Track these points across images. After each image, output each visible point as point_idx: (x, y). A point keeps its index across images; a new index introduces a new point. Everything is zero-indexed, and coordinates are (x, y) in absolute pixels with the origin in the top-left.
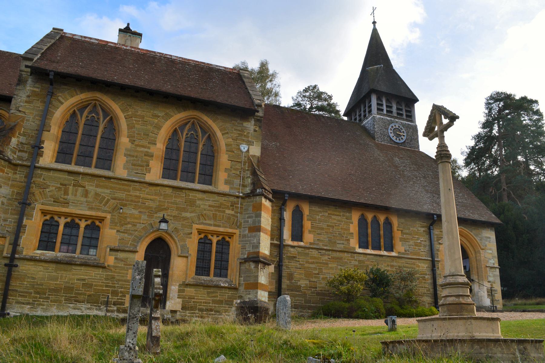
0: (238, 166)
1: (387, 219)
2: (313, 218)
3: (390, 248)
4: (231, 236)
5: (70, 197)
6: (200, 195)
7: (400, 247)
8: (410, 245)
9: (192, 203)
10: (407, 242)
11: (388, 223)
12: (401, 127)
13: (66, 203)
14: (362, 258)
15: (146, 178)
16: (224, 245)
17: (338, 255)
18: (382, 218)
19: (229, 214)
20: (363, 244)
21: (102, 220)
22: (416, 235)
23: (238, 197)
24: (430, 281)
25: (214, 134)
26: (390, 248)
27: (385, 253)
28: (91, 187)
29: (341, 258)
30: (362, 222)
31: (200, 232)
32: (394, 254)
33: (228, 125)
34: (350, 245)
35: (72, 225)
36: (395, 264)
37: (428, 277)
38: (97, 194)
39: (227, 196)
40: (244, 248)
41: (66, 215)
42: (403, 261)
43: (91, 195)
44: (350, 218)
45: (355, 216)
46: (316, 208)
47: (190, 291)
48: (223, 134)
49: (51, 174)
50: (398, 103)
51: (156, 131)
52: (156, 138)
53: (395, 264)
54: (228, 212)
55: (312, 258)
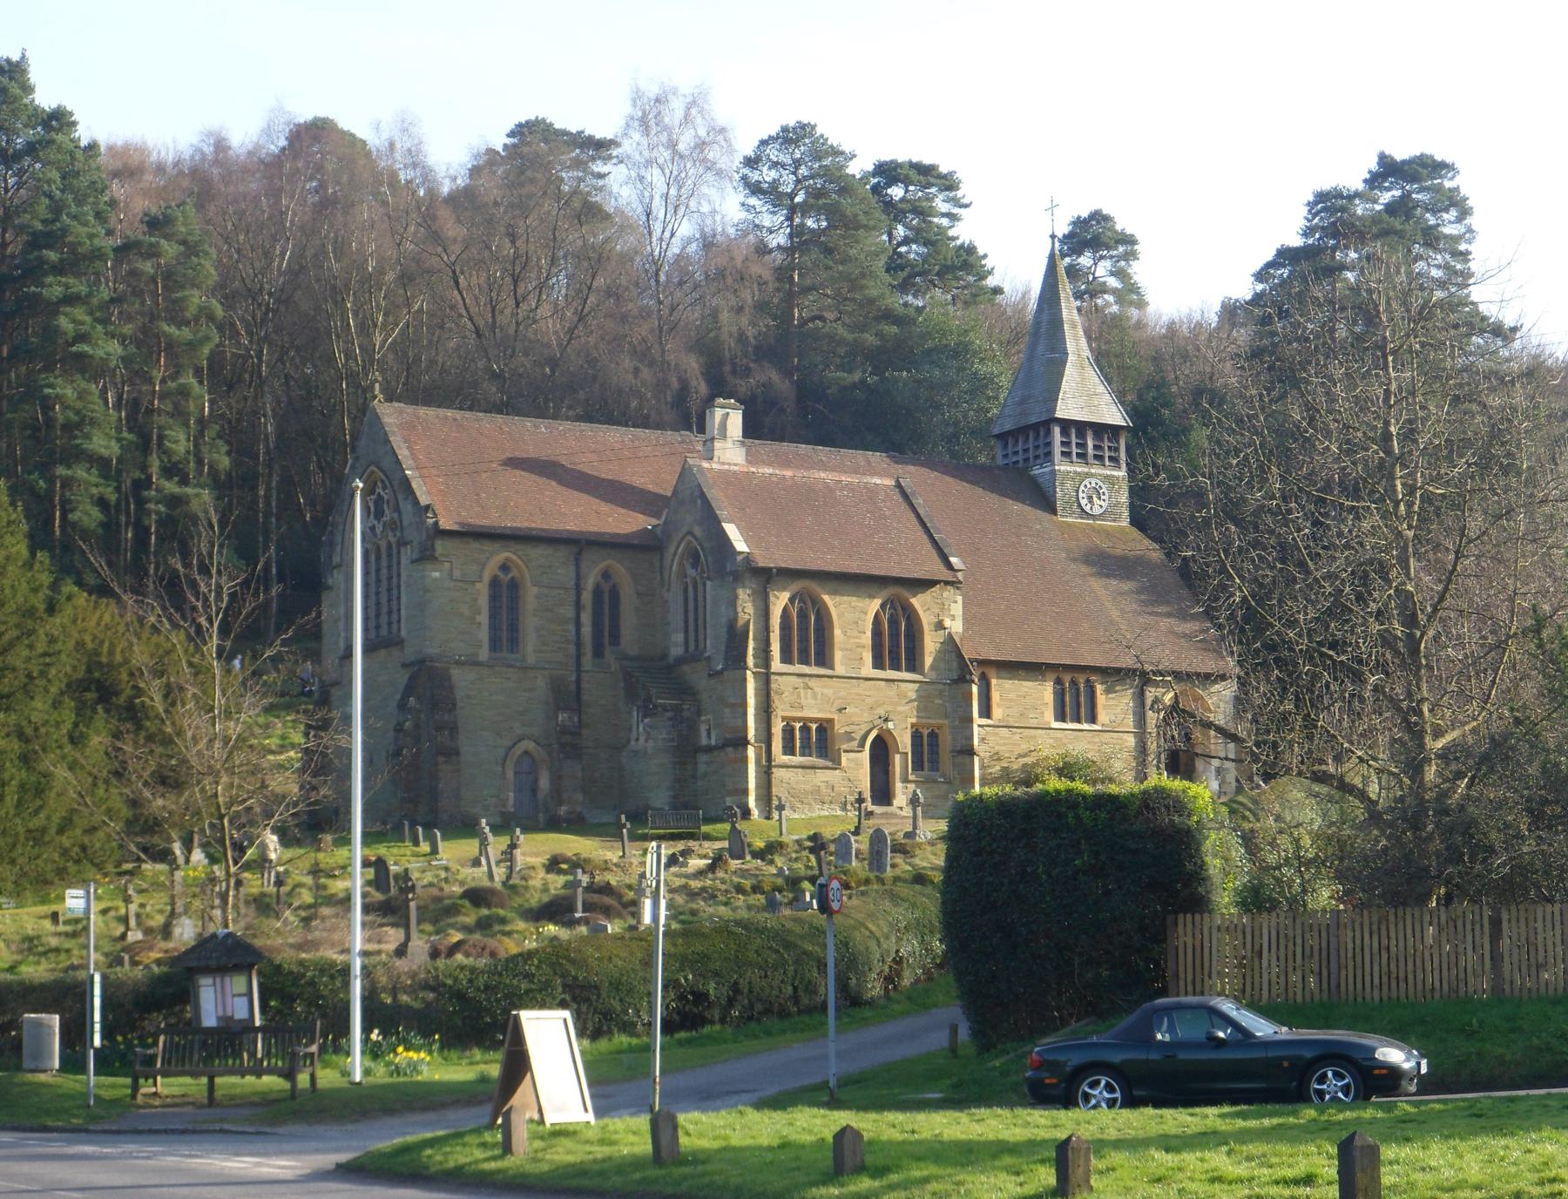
1: (1088, 681)
3: (1093, 719)
5: (803, 701)
7: (1103, 716)
12: (1100, 483)
14: (1059, 734)
16: (933, 736)
18: (1081, 680)
20: (1061, 716)
26: (1093, 719)
27: (1086, 726)
32: (1096, 727)
35: (805, 729)
36: (1096, 740)
40: (954, 739)
42: (1107, 735)
43: (819, 696)
51: (862, 616)
53: (1096, 740)
55: (1002, 738)
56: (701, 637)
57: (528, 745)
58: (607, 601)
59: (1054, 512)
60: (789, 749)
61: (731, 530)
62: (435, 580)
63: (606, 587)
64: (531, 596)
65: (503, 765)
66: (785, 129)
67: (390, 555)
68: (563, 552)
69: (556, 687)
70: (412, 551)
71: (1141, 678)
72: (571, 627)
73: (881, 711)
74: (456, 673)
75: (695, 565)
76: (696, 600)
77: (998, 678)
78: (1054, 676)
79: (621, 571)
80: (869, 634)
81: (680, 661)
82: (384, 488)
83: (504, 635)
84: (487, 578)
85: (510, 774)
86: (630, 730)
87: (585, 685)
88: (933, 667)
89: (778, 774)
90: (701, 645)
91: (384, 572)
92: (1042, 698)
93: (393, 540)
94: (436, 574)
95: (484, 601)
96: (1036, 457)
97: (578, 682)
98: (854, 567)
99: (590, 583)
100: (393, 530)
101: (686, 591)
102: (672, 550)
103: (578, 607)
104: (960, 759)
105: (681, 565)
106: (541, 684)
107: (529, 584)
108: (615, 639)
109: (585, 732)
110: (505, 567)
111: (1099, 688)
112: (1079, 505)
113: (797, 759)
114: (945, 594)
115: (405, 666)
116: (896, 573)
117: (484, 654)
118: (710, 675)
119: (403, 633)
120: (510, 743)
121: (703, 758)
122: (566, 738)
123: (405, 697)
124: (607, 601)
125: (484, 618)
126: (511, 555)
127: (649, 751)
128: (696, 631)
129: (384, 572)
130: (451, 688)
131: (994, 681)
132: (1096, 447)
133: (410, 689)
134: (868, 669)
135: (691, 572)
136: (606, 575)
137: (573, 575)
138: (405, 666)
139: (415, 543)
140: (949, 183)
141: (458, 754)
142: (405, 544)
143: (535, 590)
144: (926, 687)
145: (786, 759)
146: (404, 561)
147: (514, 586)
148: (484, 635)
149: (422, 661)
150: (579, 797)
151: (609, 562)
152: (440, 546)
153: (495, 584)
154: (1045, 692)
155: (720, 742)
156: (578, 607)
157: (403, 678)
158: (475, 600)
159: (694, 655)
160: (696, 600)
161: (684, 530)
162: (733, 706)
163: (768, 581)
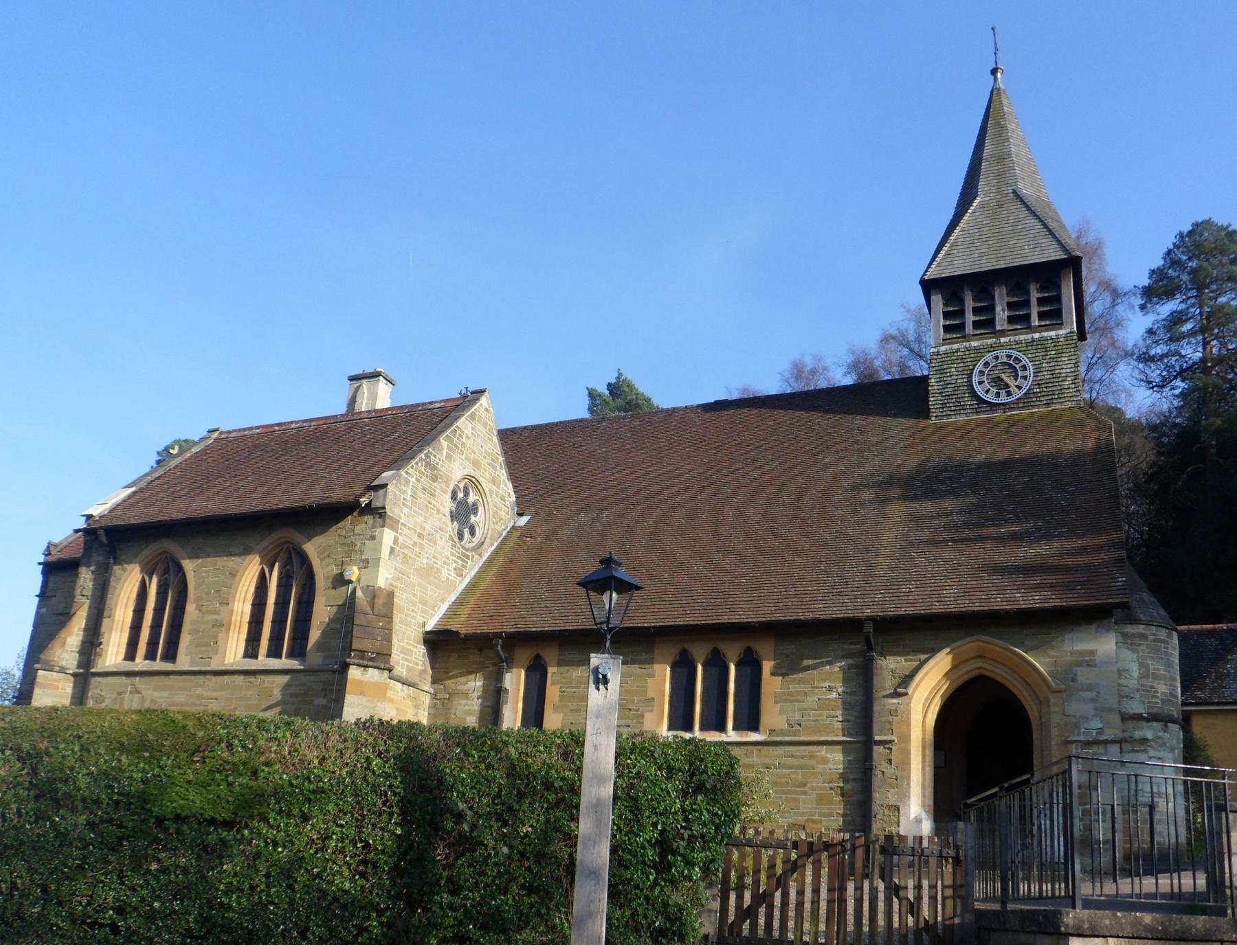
2: (564, 678)
8: (805, 709)
10: (797, 701)
15: (212, 664)
19: (318, 706)
22: (824, 680)
23: (334, 672)
34: (641, 727)
39: (319, 673)
48: (322, 560)
52: (229, 594)
59: (924, 412)
77: (561, 663)
78: (672, 651)
88: (320, 646)
111: (767, 666)
112: (974, 395)
114: (358, 529)
131: (551, 670)
144: (303, 678)
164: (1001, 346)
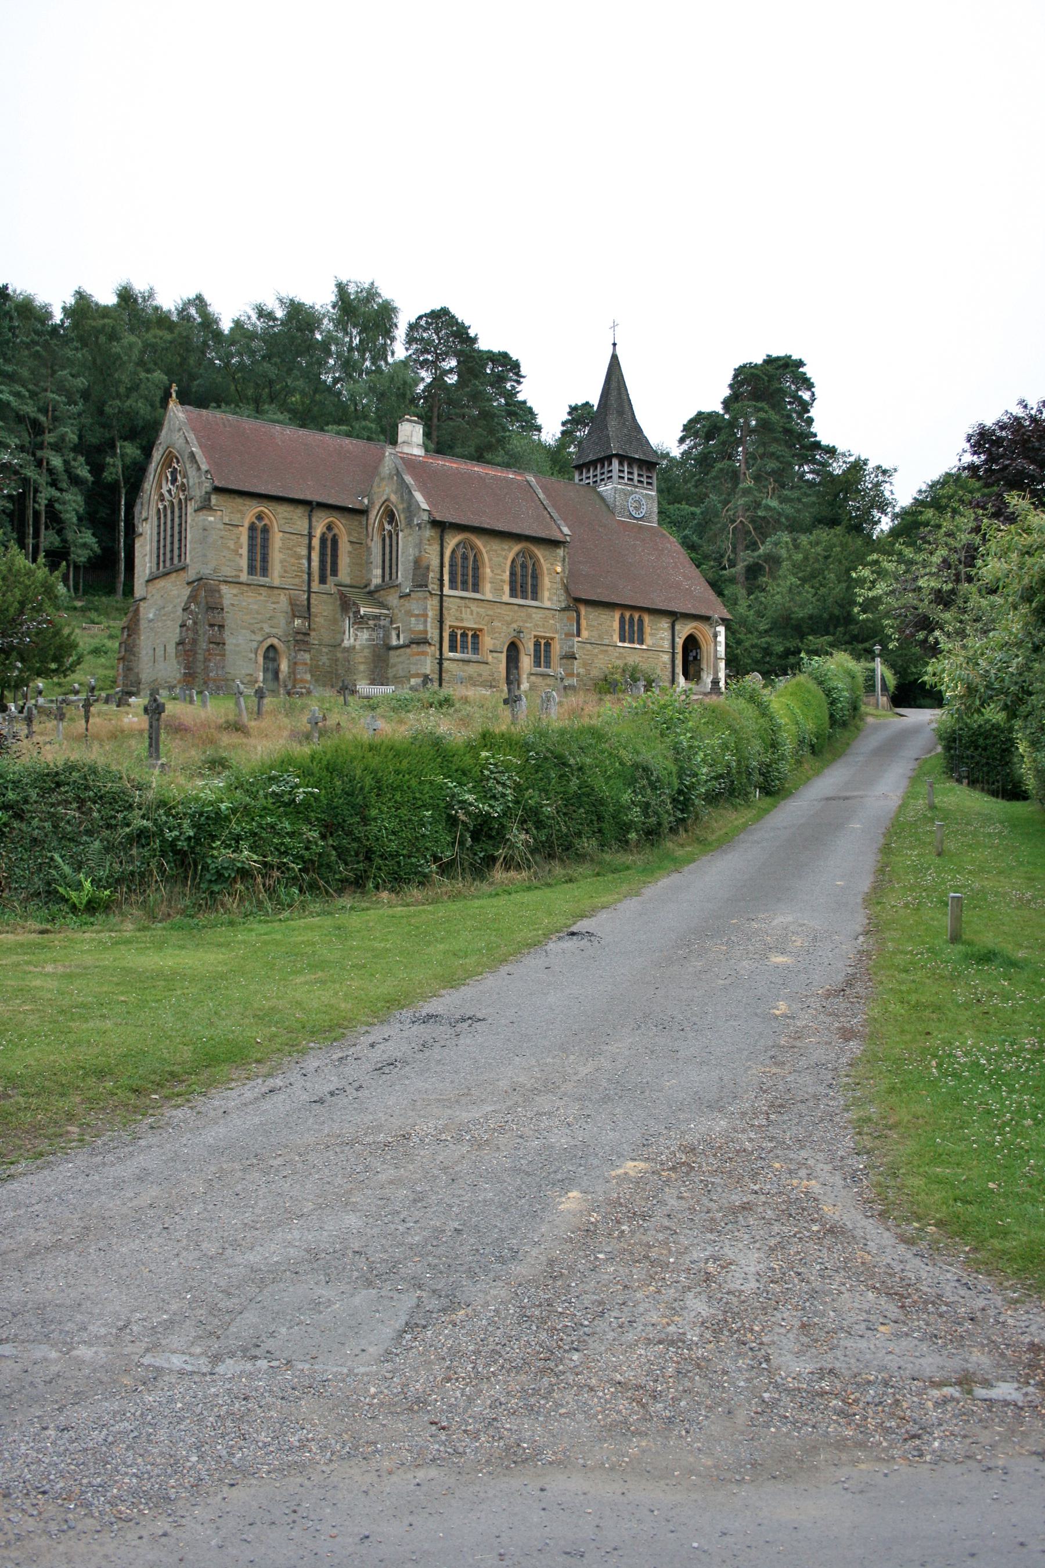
0: (555, 586)
3: (641, 642)
4: (552, 639)
5: (464, 616)
6: (534, 610)
7: (649, 640)
9: (529, 616)
11: (641, 621)
13: (462, 620)
14: (622, 650)
16: (548, 645)
17: (605, 648)
18: (636, 617)
20: (622, 639)
21: (481, 630)
24: (670, 670)
25: (538, 560)
26: (641, 642)
27: (638, 646)
28: (473, 607)
29: (606, 651)
30: (622, 617)
31: (535, 637)
32: (644, 647)
33: (547, 553)
37: (669, 666)
38: (478, 613)
40: (561, 648)
41: (461, 628)
44: (613, 617)
45: (617, 615)
46: (590, 609)
47: (533, 678)
49: (451, 599)
50: (640, 468)
54: (551, 622)
56: (394, 571)
57: (275, 641)
58: (330, 546)
60: (453, 648)
61: (418, 496)
62: (211, 522)
63: (330, 536)
64: (277, 540)
65: (256, 654)
66: (433, 312)
67: (180, 509)
68: (300, 511)
69: (292, 603)
70: (196, 502)
71: (674, 616)
72: (305, 562)
73: (515, 626)
74: (224, 588)
75: (390, 523)
76: (391, 545)
79: (342, 527)
80: (508, 573)
81: (378, 589)
82: (178, 462)
83: (258, 565)
84: (247, 524)
85: (261, 660)
86: (344, 633)
87: (312, 601)
89: (446, 664)
90: (394, 576)
91: (177, 520)
92: (612, 626)
93: (182, 497)
94: (211, 519)
95: (244, 539)
96: (602, 480)
97: (309, 599)
98: (500, 526)
99: (318, 533)
100: (183, 491)
101: (384, 540)
102: (375, 512)
103: (310, 548)
104: (564, 661)
105: (381, 522)
106: (283, 600)
107: (276, 530)
108: (335, 572)
109: (313, 634)
110: (260, 517)
113: (457, 655)
115: (189, 583)
116: (527, 533)
117: (244, 577)
118: (401, 597)
119: (188, 560)
120: (261, 639)
121: (392, 653)
122: (299, 637)
123: (188, 602)
124: (330, 546)
125: (244, 551)
126: (266, 511)
127: (357, 647)
128: (391, 567)
129: (177, 520)
130: (221, 597)
132: (639, 475)
133: (193, 598)
134: (506, 598)
135: (387, 527)
136: (329, 528)
137: (307, 526)
138: (189, 583)
139: (197, 498)
140: (516, 366)
141: (224, 644)
142: (191, 500)
143: (281, 534)
145: (451, 654)
146: (190, 510)
147: (266, 530)
148: (244, 563)
149: (201, 579)
150: (308, 677)
151: (331, 519)
152: (214, 499)
153: (252, 528)
154: (613, 621)
155: (407, 642)
156: (310, 548)
157: (187, 591)
158: (239, 538)
159: (389, 583)
160: (391, 545)
161: (384, 497)
162: (417, 616)
163: (442, 532)
164: (636, 493)
